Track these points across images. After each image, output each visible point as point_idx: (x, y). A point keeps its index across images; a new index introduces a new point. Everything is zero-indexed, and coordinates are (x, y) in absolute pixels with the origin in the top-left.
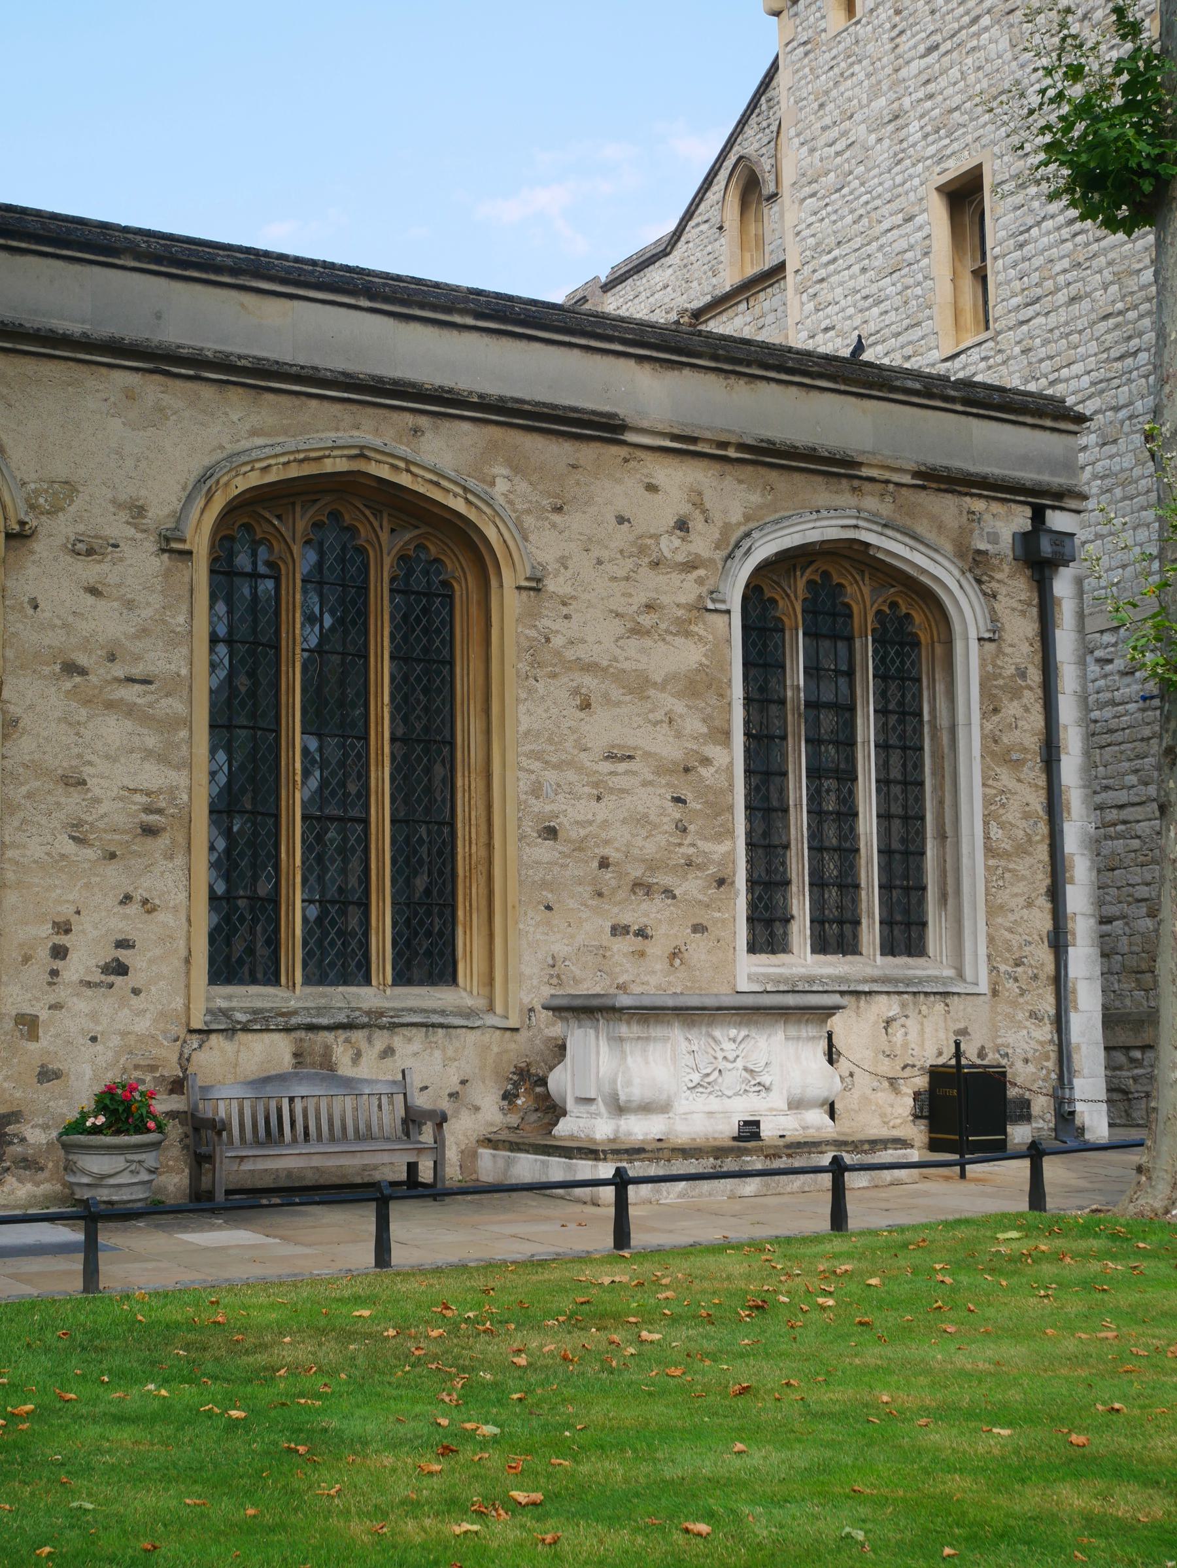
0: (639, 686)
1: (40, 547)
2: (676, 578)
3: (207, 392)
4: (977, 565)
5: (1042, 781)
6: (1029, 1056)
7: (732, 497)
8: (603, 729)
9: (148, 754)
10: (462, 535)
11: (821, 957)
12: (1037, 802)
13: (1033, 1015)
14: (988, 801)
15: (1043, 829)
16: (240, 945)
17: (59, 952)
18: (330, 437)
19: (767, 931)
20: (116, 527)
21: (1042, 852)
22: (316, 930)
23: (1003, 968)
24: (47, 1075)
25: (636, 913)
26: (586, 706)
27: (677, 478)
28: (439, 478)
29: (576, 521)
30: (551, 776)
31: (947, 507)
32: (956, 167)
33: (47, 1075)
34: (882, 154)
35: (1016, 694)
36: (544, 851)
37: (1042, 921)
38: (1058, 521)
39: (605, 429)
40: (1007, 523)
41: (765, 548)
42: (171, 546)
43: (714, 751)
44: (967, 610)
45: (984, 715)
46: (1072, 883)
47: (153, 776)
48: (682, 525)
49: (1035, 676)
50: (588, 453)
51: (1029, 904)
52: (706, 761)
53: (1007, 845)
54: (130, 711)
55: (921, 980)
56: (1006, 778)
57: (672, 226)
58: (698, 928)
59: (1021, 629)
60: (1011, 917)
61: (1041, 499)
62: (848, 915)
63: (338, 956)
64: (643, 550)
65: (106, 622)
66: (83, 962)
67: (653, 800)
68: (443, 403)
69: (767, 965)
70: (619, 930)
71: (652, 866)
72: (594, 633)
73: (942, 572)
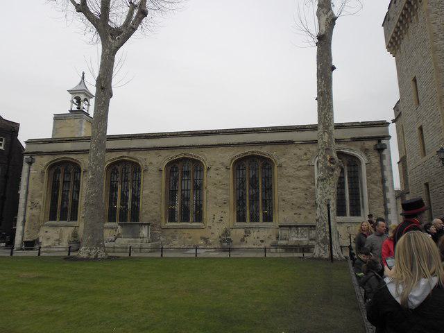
0: (299, 178)
1: (211, 170)
2: (304, 162)
3: (232, 148)
4: (366, 151)
5: (381, 186)
8: (292, 185)
9: (225, 194)
10: (269, 160)
11: (274, 220)
12: (381, 190)
14: (368, 190)
16: (241, 218)
17: (214, 219)
18: (248, 150)
20: (220, 166)
21: (382, 198)
24: (212, 233)
25: (298, 211)
26: (289, 182)
27: (304, 148)
28: (264, 154)
29: (287, 156)
30: (283, 193)
31: (359, 143)
33: (212, 233)
35: (375, 172)
36: (282, 203)
37: (383, 210)
38: (383, 142)
39: (291, 142)
40: (370, 144)
42: (227, 168)
43: (313, 187)
44: (364, 160)
45: (367, 176)
48: (306, 154)
49: (379, 168)
52: (311, 188)
54: (223, 189)
56: (373, 186)
58: (310, 213)
59: (375, 161)
61: (379, 139)
63: (254, 218)
64: (299, 158)
65: (219, 178)
66: (217, 220)
67: (302, 194)
68: (265, 143)
70: (295, 214)
71: (302, 204)
72: (291, 171)
73: (357, 154)
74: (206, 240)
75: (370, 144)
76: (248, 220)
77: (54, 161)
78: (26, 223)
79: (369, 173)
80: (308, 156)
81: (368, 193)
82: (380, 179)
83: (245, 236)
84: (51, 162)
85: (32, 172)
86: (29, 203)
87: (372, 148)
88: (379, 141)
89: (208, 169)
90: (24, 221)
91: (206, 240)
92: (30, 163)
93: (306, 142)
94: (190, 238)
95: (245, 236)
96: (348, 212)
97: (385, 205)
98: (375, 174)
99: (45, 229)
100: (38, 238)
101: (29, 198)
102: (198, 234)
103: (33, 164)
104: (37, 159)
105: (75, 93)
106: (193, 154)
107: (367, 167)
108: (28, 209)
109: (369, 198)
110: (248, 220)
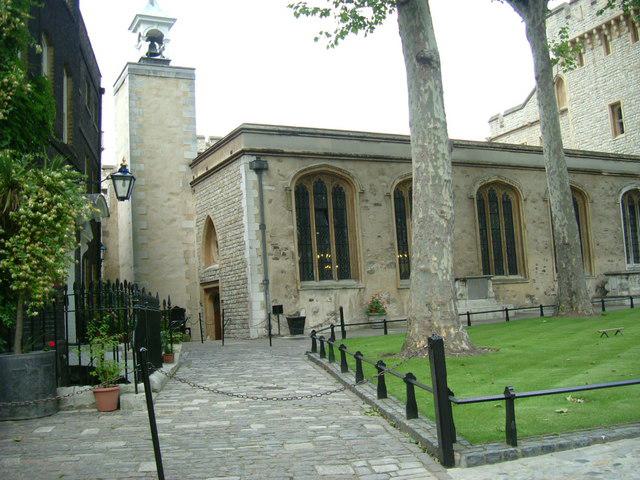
1: (528, 201)
7: (617, 182)
8: (604, 225)
19: (628, 262)
22: (339, 270)
25: (611, 257)
27: (612, 179)
32: (613, 102)
34: (594, 96)
36: (597, 248)
39: (598, 173)
41: (624, 191)
47: (546, 239)
50: (597, 177)
57: (522, 102)
65: (537, 214)
69: (628, 266)
74: (530, 297)
77: (305, 170)
78: (270, 286)
84: (301, 172)
85: (266, 188)
86: (270, 249)
89: (525, 200)
90: (266, 282)
91: (530, 297)
92: (260, 169)
93: (612, 174)
99: (305, 296)
100: (298, 313)
101: (268, 238)
102: (521, 289)
103: (264, 174)
104: (272, 163)
105: (152, 23)
106: (508, 176)
108: (270, 258)
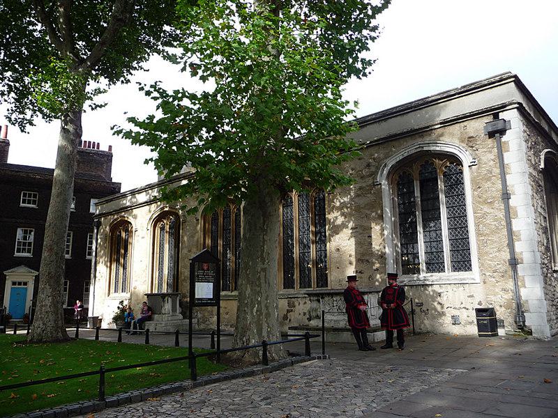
4: (470, 141)
6: (502, 304)
12: (501, 215)
13: (504, 290)
14: (475, 217)
15: (504, 223)
21: (505, 232)
23: (488, 274)
35: (489, 179)
40: (478, 127)
44: (466, 159)
46: (519, 240)
49: (497, 171)
51: (499, 251)
53: (487, 232)
55: (464, 279)
56: (486, 209)
60: (491, 256)
62: (416, 262)
75: (478, 127)
76: (297, 285)
79: (477, 186)
80: (373, 169)
81: (477, 225)
82: (499, 194)
83: (288, 311)
87: (482, 134)
88: (496, 116)
94: (227, 313)
95: (288, 311)
96: (423, 266)
97: (511, 246)
98: (489, 184)
107: (472, 173)
109: (479, 234)
110: (297, 285)
